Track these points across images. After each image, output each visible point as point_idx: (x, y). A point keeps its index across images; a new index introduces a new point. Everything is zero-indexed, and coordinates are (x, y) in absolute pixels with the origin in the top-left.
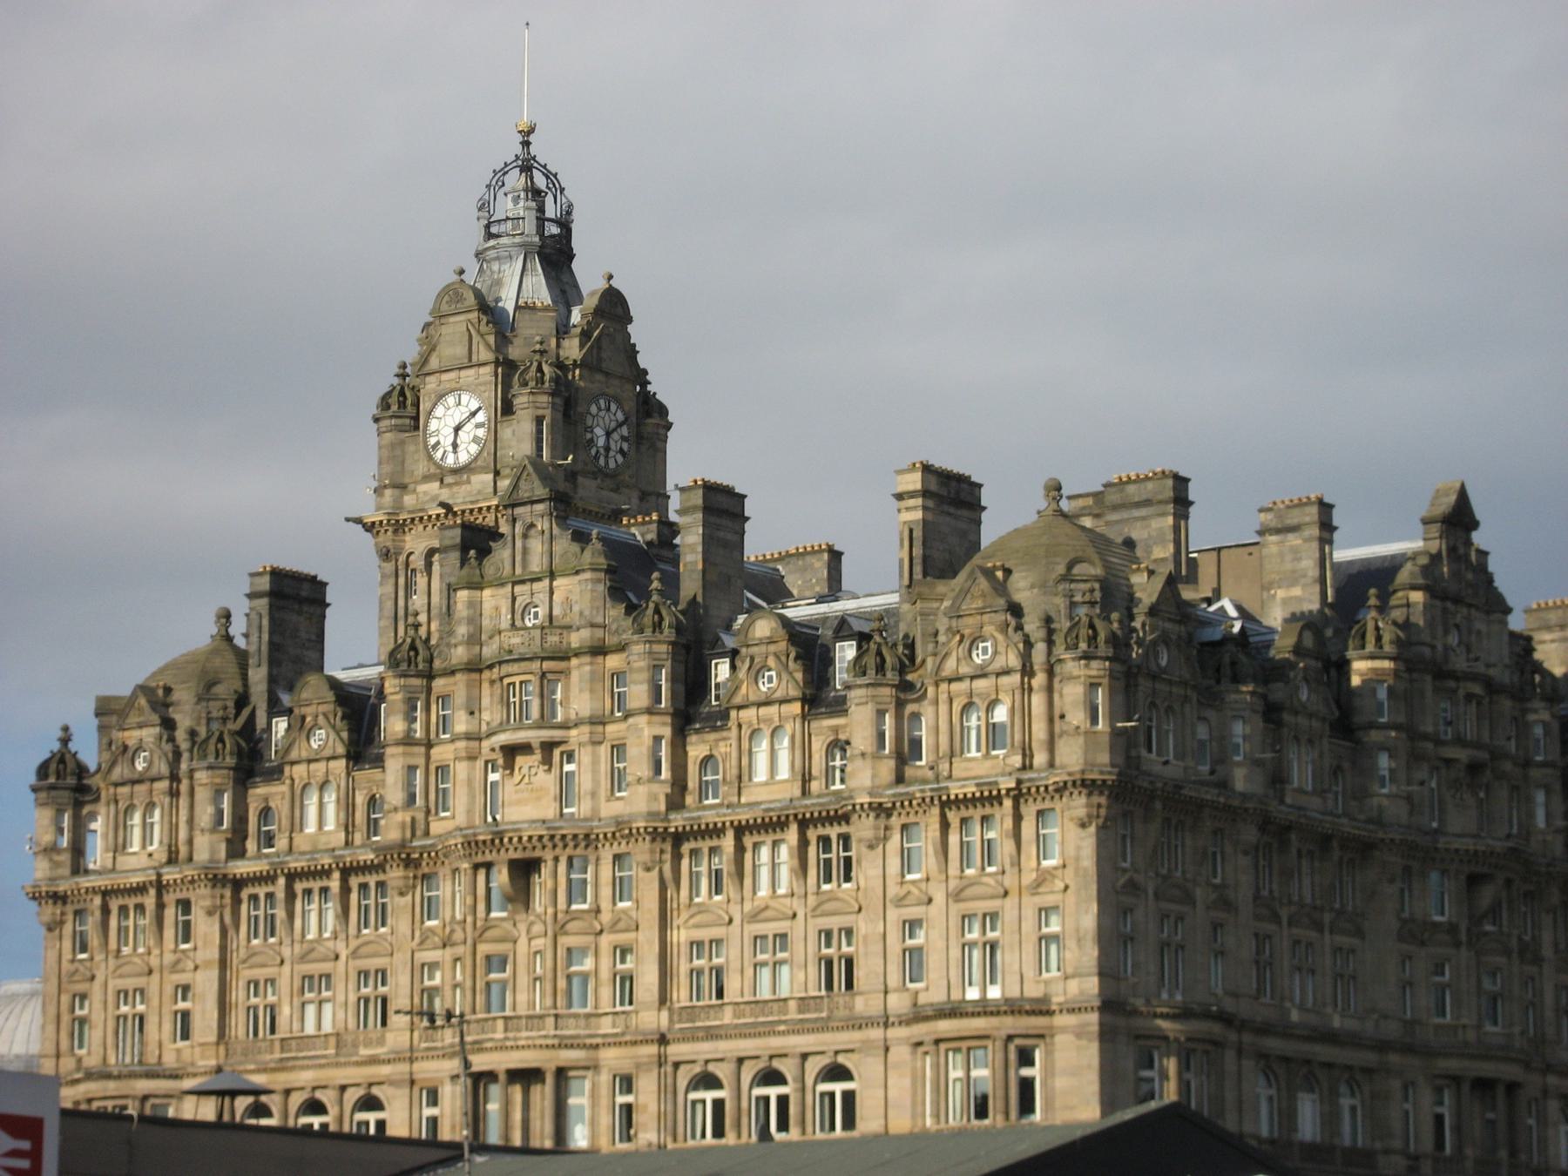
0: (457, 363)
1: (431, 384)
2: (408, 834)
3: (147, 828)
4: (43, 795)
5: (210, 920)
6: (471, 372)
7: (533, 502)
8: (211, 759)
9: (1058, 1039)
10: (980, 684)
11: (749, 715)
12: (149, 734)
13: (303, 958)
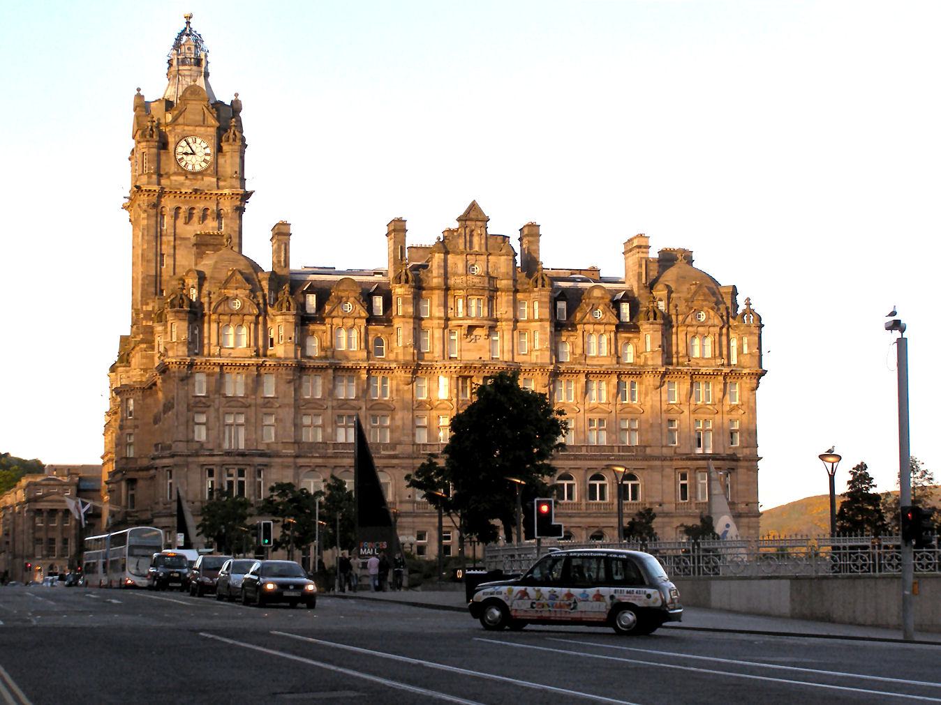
0: (197, 124)
1: (179, 129)
2: (416, 359)
3: (237, 336)
4: (182, 315)
5: (287, 385)
6: (203, 129)
7: (478, 220)
8: (284, 310)
9: (740, 470)
10: (701, 329)
11: (589, 327)
12: (242, 293)
13: (340, 407)
